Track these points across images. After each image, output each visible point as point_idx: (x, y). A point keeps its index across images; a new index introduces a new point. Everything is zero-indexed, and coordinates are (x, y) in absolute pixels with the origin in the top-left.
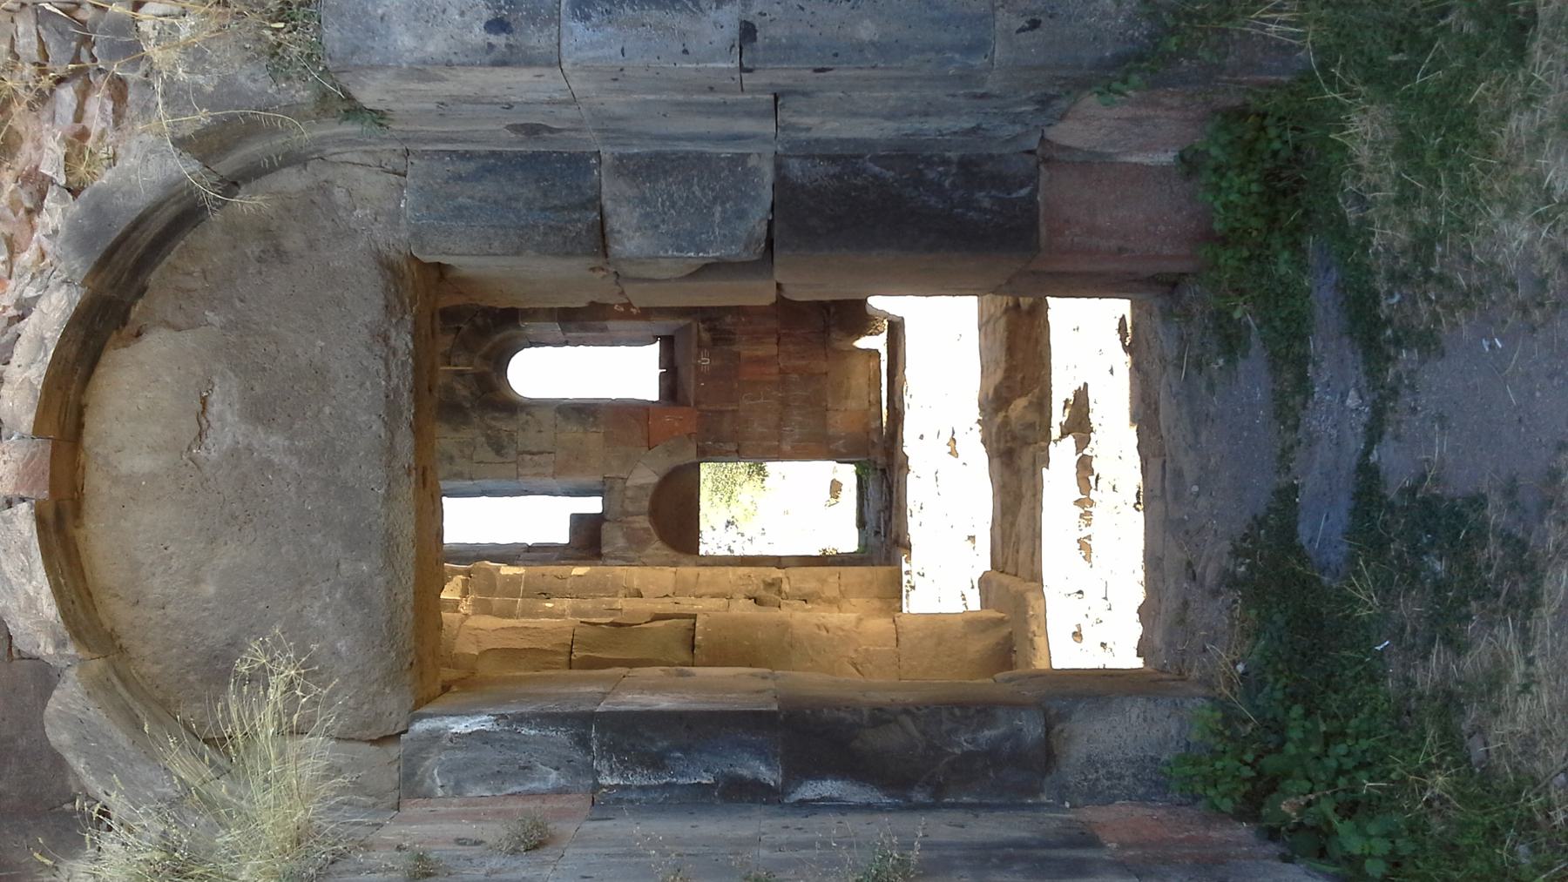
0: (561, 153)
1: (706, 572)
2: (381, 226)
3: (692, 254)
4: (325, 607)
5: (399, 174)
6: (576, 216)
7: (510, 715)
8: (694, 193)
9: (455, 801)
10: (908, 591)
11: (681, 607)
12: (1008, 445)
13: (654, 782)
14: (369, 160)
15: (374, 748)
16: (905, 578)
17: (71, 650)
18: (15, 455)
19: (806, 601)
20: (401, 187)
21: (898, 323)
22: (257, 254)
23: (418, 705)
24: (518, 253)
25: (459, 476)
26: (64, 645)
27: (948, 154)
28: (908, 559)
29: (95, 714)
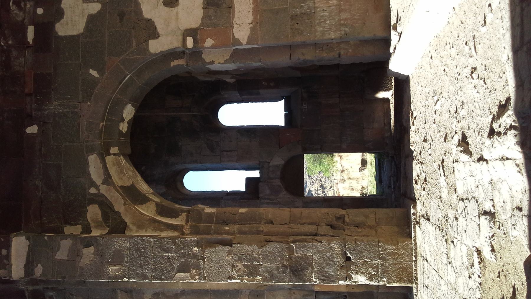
1: (306, 211)
10: (414, 224)
11: (293, 230)
16: (413, 217)
19: (358, 227)
25: (196, 162)
28: (415, 207)
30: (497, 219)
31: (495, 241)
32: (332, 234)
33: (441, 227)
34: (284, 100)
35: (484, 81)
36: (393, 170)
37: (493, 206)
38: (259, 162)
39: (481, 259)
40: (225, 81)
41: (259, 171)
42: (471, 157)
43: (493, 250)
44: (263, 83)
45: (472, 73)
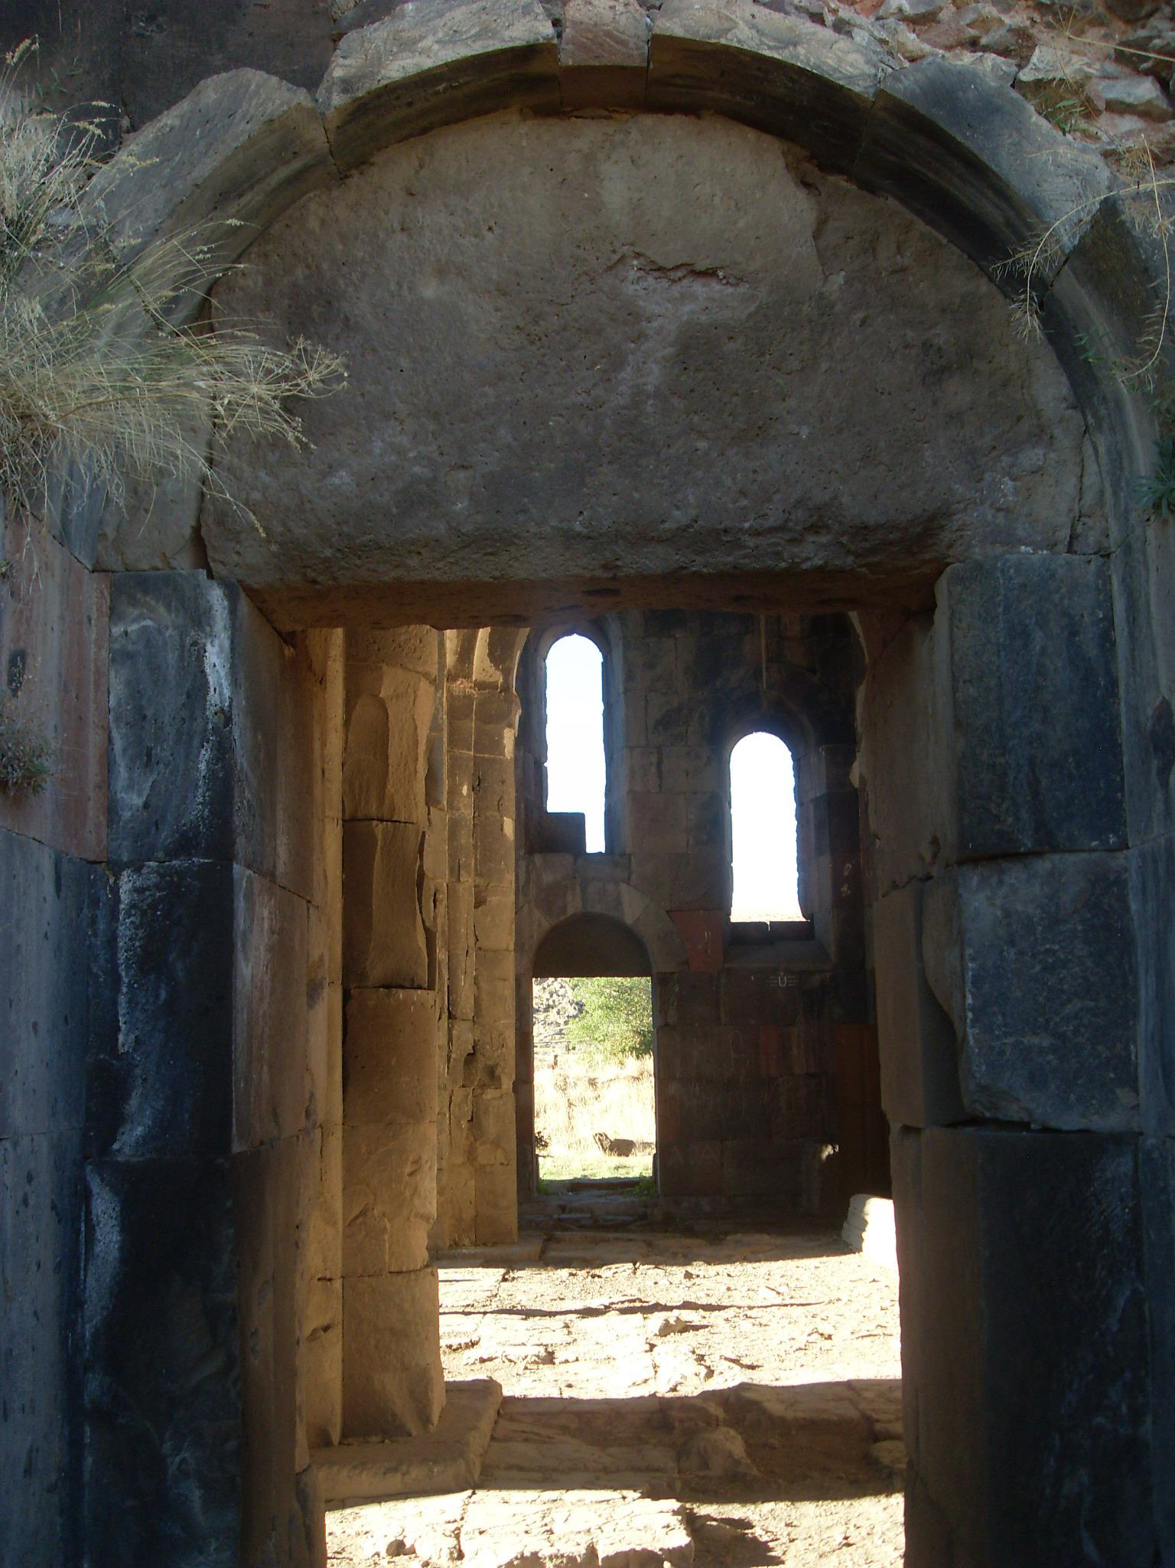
0: (1122, 790)
1: (508, 990)
2: (990, 518)
3: (969, 1000)
4: (401, 452)
5: (1070, 544)
6: (1024, 814)
7: (230, 732)
8: (1069, 1001)
9: (104, 653)
12: (677, 1424)
13: (122, 956)
14: (1089, 498)
15: (187, 532)
17: (338, 100)
18: (623, 20)
20: (1052, 546)
21: (839, 1235)
22: (936, 341)
23: (252, 593)
24: (958, 724)
25: (629, 677)
26: (345, 91)
27: (1149, 1420)
29: (242, 130)
30: (541, 1366)
31: (502, 1363)
32: (454, 1056)
33: (496, 1299)
34: (804, 920)
35: (800, 1349)
36: (610, 1217)
37: (567, 1361)
38: (630, 855)
39: (457, 1349)
40: (854, 758)
41: (604, 851)
42: (656, 1335)
43: (482, 1361)
44: (849, 865)
45: (822, 1335)
